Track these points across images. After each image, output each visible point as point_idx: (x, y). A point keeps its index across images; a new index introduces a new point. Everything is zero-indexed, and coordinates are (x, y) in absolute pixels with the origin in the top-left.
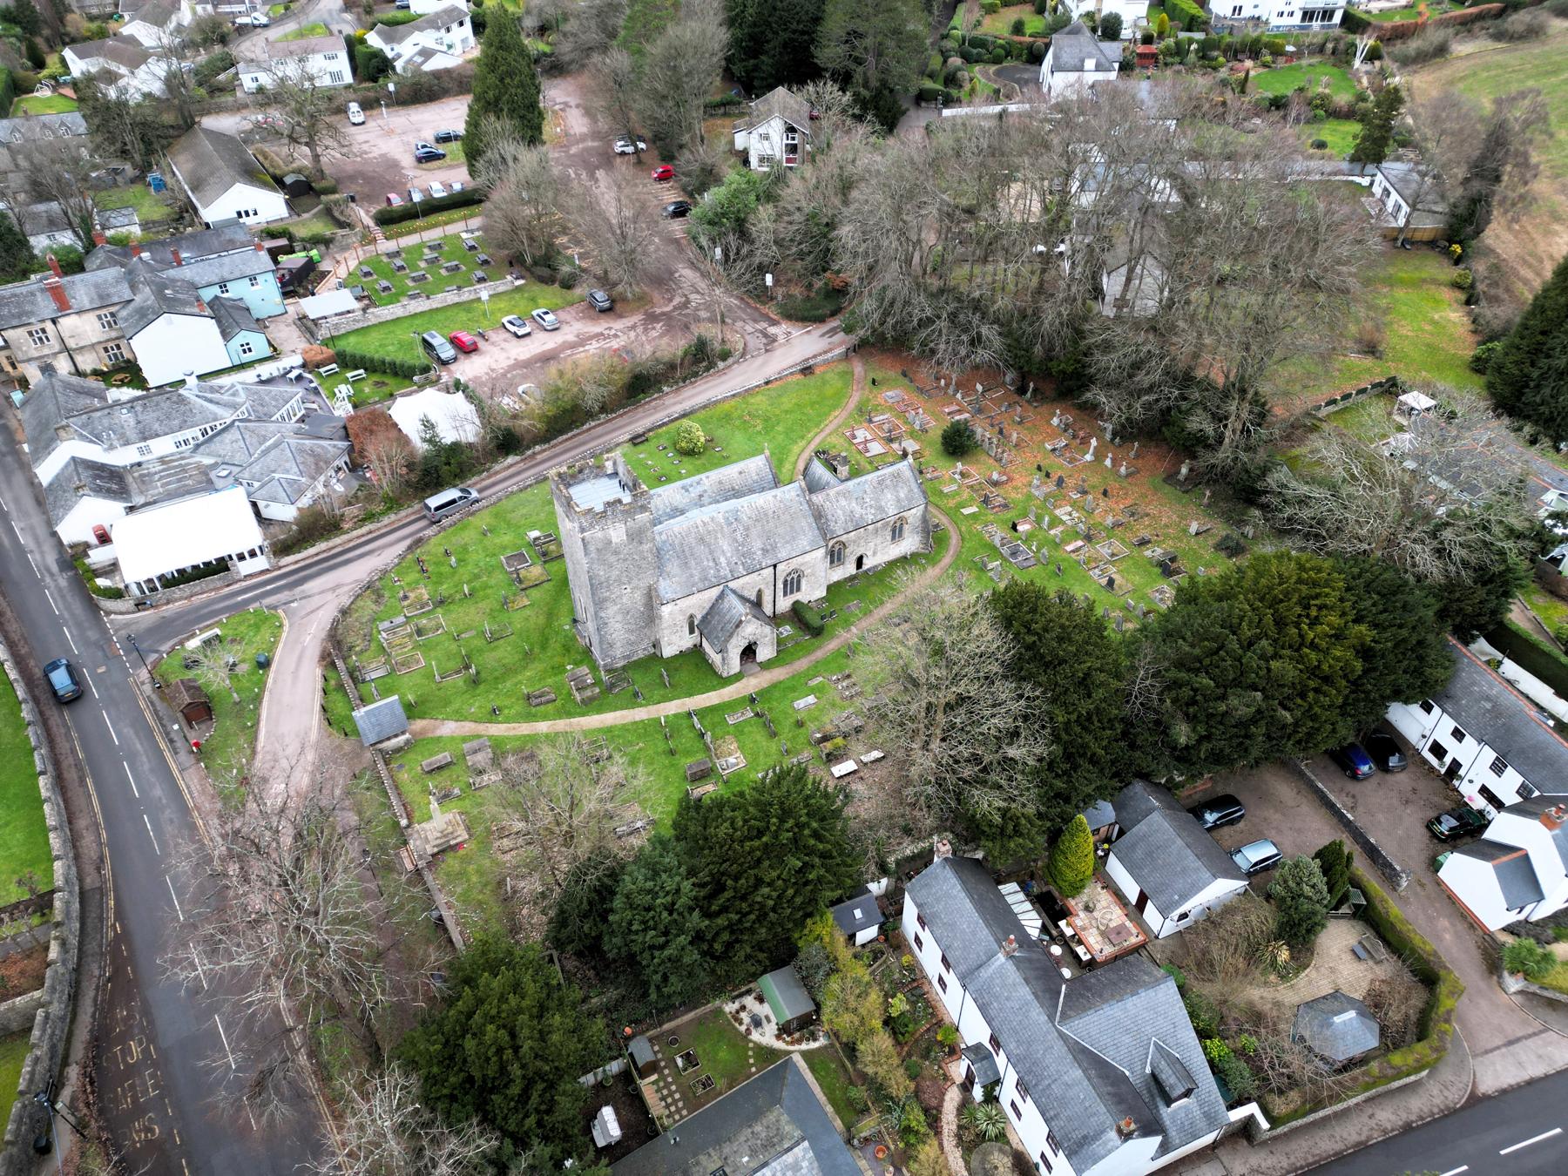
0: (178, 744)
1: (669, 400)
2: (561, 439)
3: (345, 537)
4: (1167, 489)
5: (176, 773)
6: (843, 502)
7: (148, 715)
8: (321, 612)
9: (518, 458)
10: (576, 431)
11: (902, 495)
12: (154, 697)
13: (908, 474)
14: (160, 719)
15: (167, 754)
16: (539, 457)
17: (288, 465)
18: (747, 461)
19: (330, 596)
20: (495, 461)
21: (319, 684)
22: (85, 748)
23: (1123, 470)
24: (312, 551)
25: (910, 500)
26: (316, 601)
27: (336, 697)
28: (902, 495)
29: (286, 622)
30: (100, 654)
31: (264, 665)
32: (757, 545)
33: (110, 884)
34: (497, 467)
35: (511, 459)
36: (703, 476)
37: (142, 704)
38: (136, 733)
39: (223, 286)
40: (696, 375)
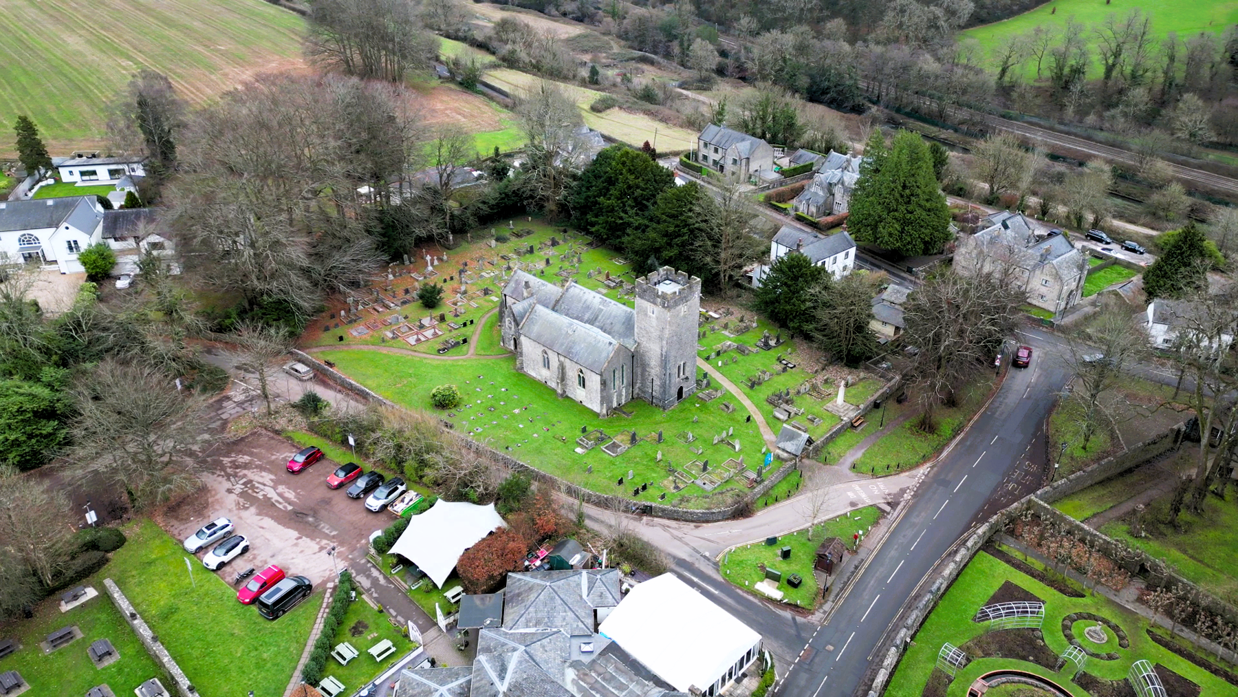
0: (856, 563)
4: (458, 249)
5: (875, 553)
7: (846, 594)
8: (706, 536)
12: (831, 598)
14: (845, 583)
15: (866, 565)
17: (573, 584)
19: (687, 539)
21: (771, 508)
22: (897, 611)
23: (445, 258)
26: (697, 544)
27: (774, 493)
29: (728, 549)
30: (817, 660)
31: (772, 542)
33: (958, 541)
37: (842, 601)
38: (864, 590)
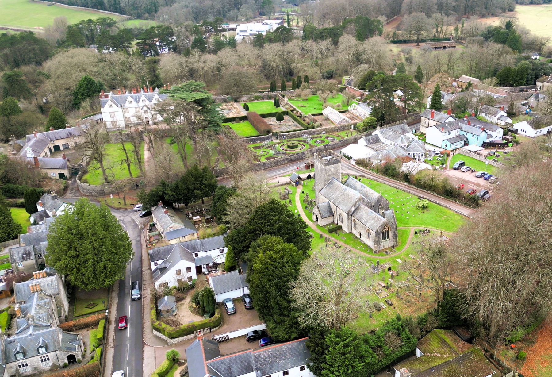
1: (453, 204)
2: (421, 189)
3: (366, 170)
6: (364, 213)
9: (408, 185)
10: (425, 191)
11: (374, 225)
13: (382, 222)
16: (411, 188)
18: (376, 193)
20: (402, 180)
24: (361, 168)
25: (374, 227)
28: (374, 225)
32: (340, 199)
34: (402, 182)
35: (406, 183)
36: (367, 187)
39: (467, 133)
40: (470, 206)
